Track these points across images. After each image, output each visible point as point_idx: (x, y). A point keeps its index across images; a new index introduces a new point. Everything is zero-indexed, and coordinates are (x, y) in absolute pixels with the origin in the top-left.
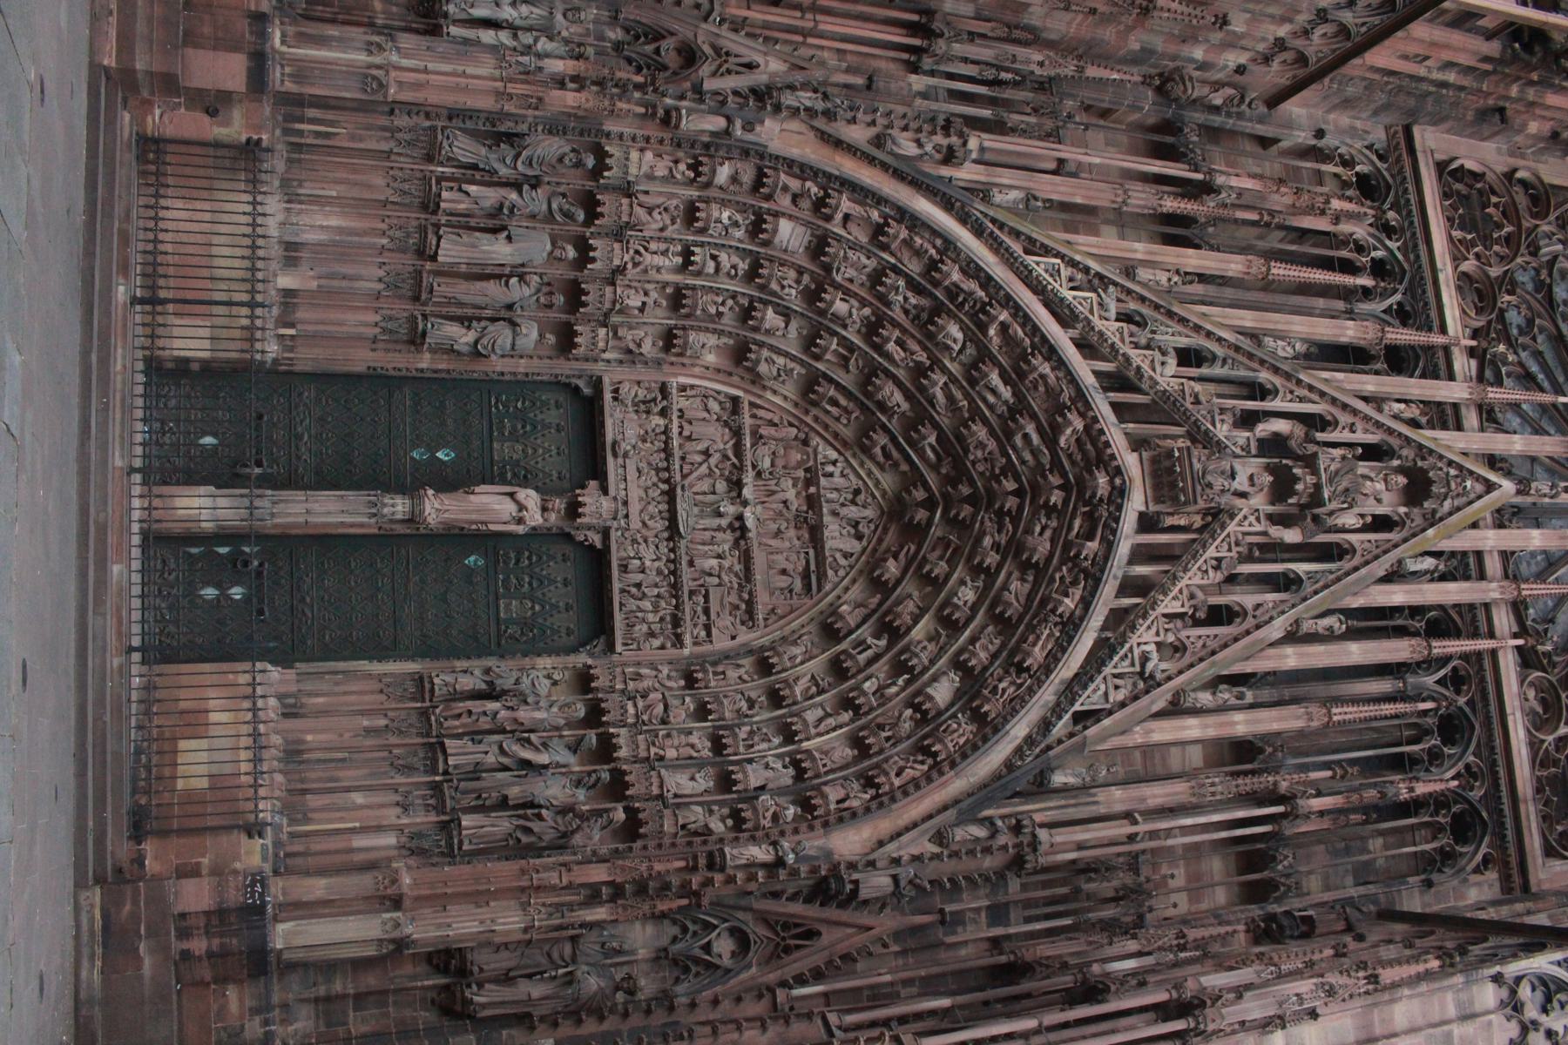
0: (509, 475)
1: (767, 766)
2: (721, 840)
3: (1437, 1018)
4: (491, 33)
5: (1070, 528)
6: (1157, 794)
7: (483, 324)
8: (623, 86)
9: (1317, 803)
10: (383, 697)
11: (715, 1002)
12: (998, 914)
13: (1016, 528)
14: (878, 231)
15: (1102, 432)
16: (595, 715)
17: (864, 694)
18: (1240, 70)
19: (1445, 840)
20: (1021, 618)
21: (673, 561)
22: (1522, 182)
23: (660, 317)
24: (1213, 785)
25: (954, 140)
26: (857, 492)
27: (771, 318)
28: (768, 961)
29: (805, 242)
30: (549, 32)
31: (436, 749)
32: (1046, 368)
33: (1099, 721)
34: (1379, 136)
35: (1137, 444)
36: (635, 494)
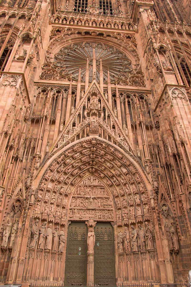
0: (84, 237)
1: (136, 198)
2: (150, 207)
3: (178, 108)
4: (12, 238)
5: (100, 148)
6: (140, 141)
7: (60, 241)
8: (25, 213)
9: (141, 118)
10: (123, 262)
11: (174, 210)
12: (157, 166)
13: (98, 155)
14: (51, 171)
15: (86, 140)
16: (126, 225)
17: (124, 182)
18: (25, 107)
19: (144, 101)
20: (113, 157)
21: (99, 210)
22: (43, 67)
23: (60, 209)
24: (139, 133)
25: (37, 156)
26: (88, 179)
27: (62, 190)
28: (167, 201)
29: (51, 183)
30: (12, 226)
31: (134, 253)
32: (76, 147)
33: (130, 148)
34: (36, 87)
35: (88, 135)
36: (88, 215)
